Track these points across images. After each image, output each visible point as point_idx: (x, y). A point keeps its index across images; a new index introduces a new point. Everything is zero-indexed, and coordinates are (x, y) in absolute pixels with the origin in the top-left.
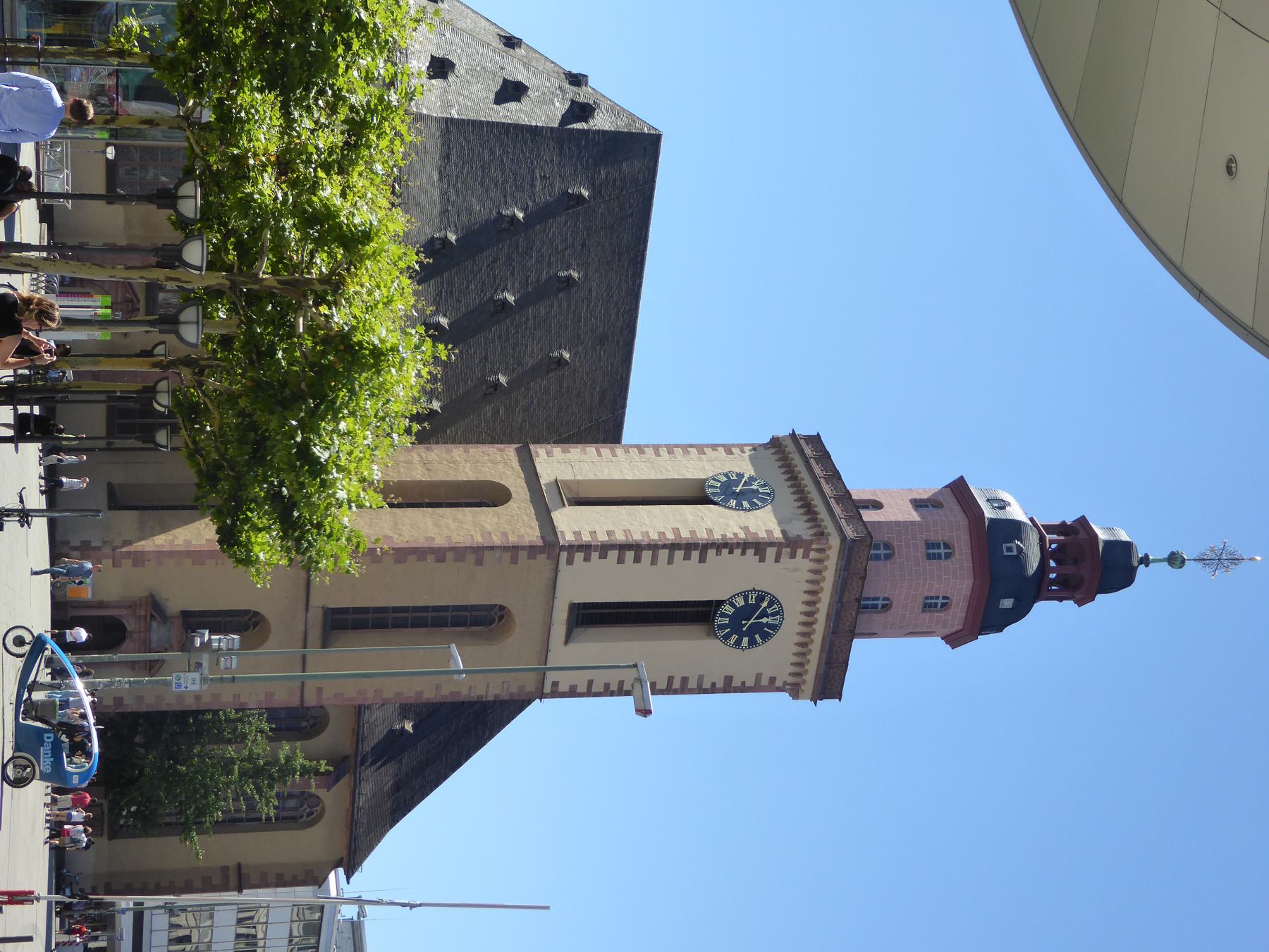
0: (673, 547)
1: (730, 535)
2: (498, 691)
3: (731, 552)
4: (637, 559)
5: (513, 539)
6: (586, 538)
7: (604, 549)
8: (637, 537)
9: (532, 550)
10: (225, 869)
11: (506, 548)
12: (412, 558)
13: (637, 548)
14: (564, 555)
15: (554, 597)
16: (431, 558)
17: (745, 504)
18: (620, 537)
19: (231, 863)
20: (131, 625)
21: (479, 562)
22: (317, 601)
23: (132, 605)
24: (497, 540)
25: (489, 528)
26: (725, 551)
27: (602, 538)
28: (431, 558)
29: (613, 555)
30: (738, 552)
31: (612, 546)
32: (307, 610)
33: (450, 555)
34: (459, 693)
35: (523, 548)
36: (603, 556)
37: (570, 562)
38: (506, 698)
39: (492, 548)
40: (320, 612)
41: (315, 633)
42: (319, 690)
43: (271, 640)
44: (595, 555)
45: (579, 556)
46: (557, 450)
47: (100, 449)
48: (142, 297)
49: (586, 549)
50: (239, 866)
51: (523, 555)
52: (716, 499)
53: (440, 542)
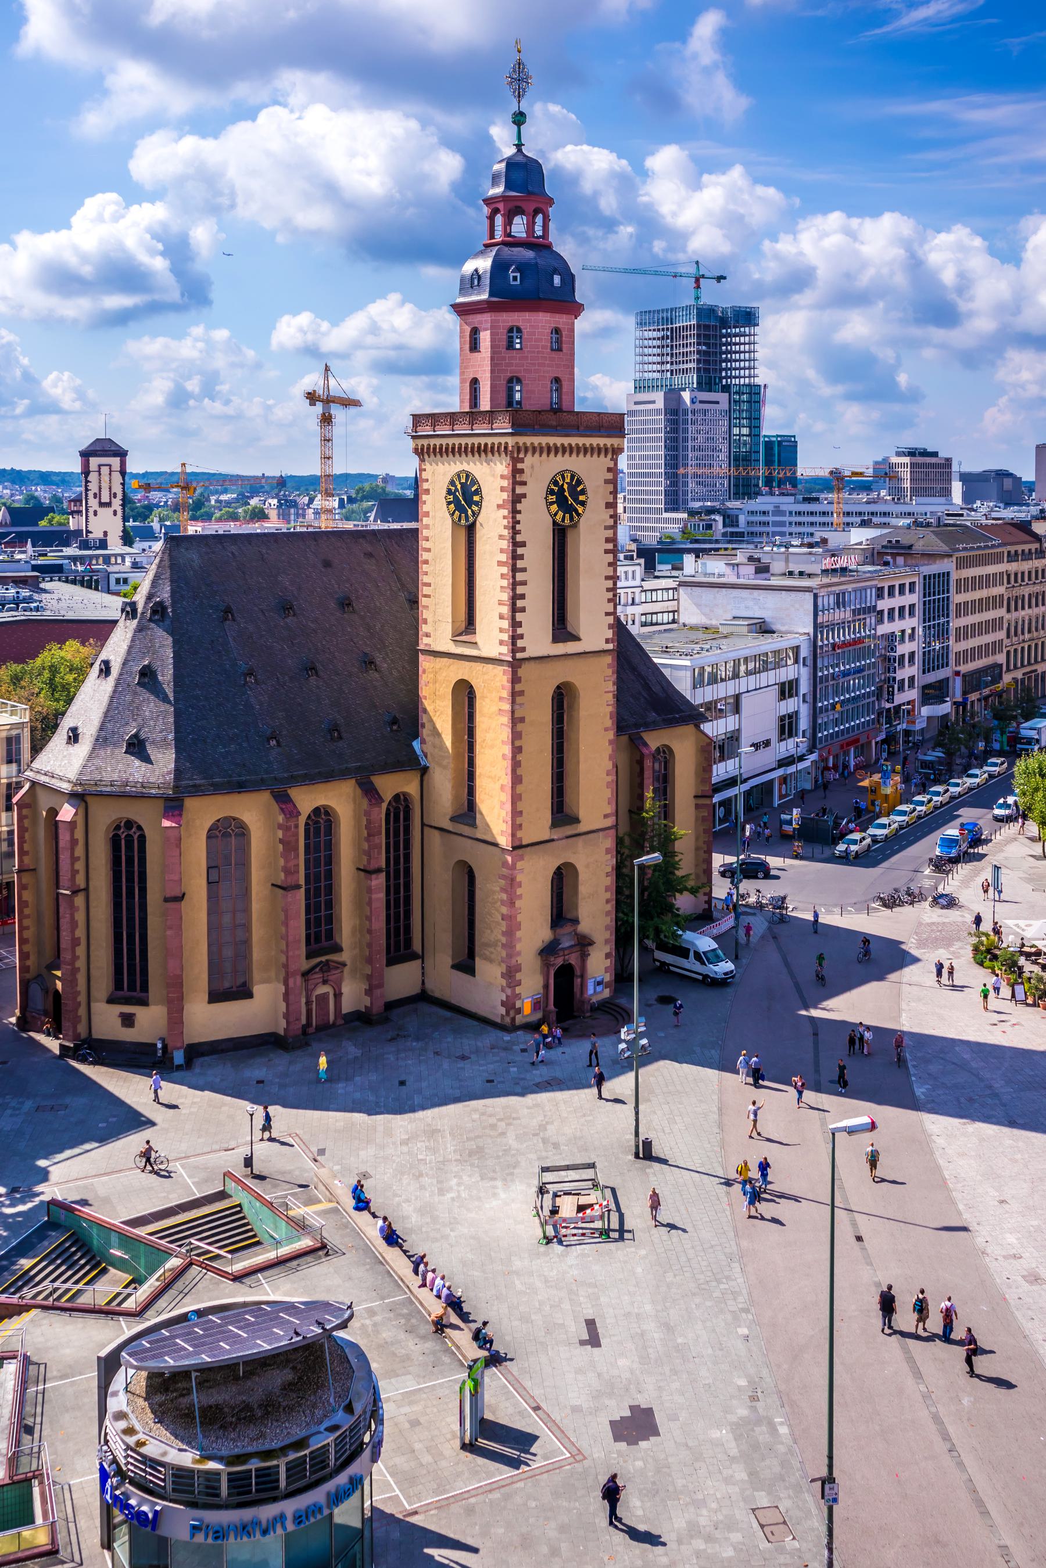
0: (514, 570)
1: (505, 522)
2: (611, 683)
3: (518, 522)
4: (522, 597)
5: (506, 694)
6: (505, 637)
7: (515, 624)
8: (505, 597)
9: (515, 680)
10: (697, 806)
11: (513, 702)
12: (519, 772)
13: (515, 597)
14: (519, 655)
15: (549, 657)
16: (519, 757)
17: (476, 498)
18: (505, 610)
19: (692, 802)
20: (559, 961)
21: (522, 720)
22: (546, 836)
23: (546, 965)
24: (507, 707)
25: (494, 709)
26: (518, 527)
27: (505, 624)
28: (519, 757)
29: (519, 617)
30: (518, 517)
31: (513, 618)
32: (553, 840)
33: (518, 743)
34: (611, 713)
35: (513, 688)
36: (520, 624)
37: (523, 649)
38: (615, 676)
39: (513, 712)
40: (554, 830)
41: (569, 830)
42: (606, 816)
43: (572, 860)
44: (519, 631)
45: (520, 643)
46: (424, 628)
47: (423, 962)
48: (318, 960)
49: (514, 638)
50: (696, 797)
51: (518, 687)
52: (471, 519)
53: (507, 750)
